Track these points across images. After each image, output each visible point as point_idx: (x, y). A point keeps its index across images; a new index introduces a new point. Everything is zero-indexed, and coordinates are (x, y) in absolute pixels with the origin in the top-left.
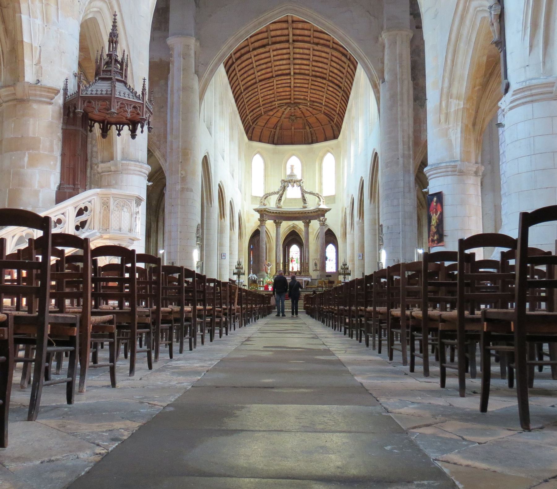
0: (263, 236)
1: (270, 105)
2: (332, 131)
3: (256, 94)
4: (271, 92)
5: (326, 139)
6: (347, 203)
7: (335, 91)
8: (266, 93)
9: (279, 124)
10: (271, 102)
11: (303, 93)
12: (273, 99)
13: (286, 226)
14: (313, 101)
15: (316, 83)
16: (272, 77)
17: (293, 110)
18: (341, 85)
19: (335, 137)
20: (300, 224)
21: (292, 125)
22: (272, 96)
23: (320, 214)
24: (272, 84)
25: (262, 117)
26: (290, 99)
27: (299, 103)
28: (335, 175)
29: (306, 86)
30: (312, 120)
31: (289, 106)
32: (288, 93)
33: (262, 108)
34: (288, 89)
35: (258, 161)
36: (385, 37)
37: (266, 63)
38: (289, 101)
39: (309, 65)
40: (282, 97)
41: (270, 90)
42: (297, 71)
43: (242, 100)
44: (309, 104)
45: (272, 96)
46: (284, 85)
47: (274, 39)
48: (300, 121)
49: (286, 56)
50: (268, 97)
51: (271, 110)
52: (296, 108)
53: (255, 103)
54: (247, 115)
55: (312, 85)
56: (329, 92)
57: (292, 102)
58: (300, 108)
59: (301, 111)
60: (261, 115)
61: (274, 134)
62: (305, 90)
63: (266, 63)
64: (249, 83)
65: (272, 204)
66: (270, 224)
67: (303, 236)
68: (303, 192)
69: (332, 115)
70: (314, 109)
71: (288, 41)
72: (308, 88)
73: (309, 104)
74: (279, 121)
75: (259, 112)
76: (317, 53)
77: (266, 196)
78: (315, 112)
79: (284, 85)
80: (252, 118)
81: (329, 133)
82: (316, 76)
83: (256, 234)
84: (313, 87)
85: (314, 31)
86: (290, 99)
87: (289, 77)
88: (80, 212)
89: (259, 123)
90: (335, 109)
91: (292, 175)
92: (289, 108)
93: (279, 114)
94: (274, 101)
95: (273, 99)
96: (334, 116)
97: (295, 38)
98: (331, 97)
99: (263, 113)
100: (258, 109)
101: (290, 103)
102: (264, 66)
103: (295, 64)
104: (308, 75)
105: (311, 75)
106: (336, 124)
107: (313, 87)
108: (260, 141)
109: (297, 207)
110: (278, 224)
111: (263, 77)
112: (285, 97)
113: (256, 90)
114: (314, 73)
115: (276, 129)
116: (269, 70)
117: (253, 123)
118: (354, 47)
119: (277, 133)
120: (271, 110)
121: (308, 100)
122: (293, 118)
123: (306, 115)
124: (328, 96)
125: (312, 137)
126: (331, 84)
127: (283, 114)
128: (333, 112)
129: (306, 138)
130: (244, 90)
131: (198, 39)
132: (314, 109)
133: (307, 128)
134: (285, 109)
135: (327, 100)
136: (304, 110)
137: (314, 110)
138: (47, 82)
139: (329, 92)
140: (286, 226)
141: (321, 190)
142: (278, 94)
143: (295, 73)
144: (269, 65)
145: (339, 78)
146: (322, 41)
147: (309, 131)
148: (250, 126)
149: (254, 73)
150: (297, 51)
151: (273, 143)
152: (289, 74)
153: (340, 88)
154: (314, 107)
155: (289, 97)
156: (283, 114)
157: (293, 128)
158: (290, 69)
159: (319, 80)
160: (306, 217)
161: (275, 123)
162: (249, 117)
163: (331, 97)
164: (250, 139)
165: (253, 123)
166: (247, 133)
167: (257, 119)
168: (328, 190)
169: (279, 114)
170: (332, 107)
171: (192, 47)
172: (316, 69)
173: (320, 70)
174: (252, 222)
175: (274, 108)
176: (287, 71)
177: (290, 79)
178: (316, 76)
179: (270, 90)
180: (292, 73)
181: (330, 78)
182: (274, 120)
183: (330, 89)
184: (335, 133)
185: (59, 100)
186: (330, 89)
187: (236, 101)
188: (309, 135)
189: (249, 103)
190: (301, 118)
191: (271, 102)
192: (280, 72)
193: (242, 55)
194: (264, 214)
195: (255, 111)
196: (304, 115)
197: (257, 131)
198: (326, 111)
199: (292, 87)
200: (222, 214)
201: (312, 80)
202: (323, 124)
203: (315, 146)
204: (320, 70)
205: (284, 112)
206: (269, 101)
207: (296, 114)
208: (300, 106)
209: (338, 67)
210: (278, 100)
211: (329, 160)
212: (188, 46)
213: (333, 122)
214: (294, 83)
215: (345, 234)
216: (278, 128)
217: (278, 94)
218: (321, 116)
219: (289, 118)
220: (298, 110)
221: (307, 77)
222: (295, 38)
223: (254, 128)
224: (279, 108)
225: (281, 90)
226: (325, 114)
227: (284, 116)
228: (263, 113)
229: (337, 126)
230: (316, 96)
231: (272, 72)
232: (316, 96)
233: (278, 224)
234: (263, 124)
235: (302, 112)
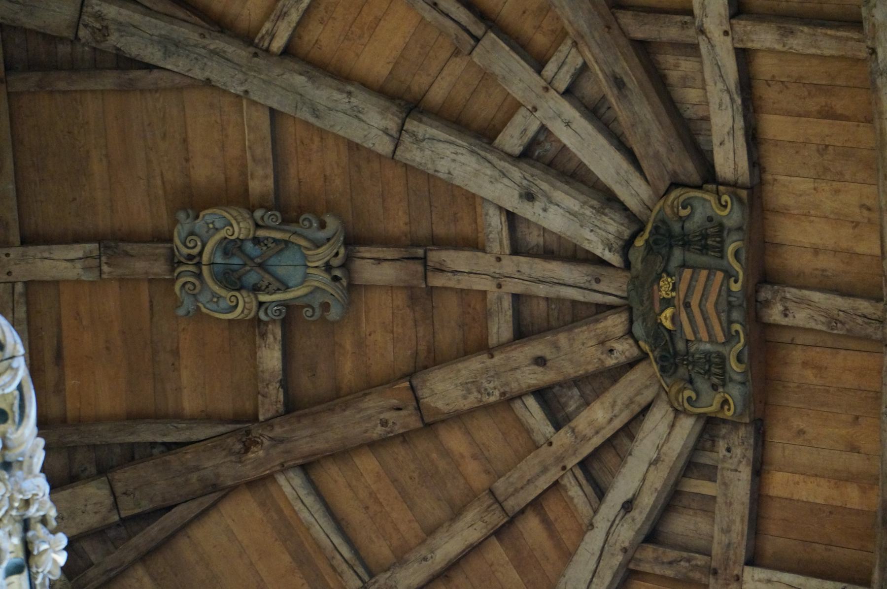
21: (112, 242)
122: (304, 273)
134: (543, 158)
156: (411, 106)
157: (60, 263)
190: (292, 407)
227: (373, 126)
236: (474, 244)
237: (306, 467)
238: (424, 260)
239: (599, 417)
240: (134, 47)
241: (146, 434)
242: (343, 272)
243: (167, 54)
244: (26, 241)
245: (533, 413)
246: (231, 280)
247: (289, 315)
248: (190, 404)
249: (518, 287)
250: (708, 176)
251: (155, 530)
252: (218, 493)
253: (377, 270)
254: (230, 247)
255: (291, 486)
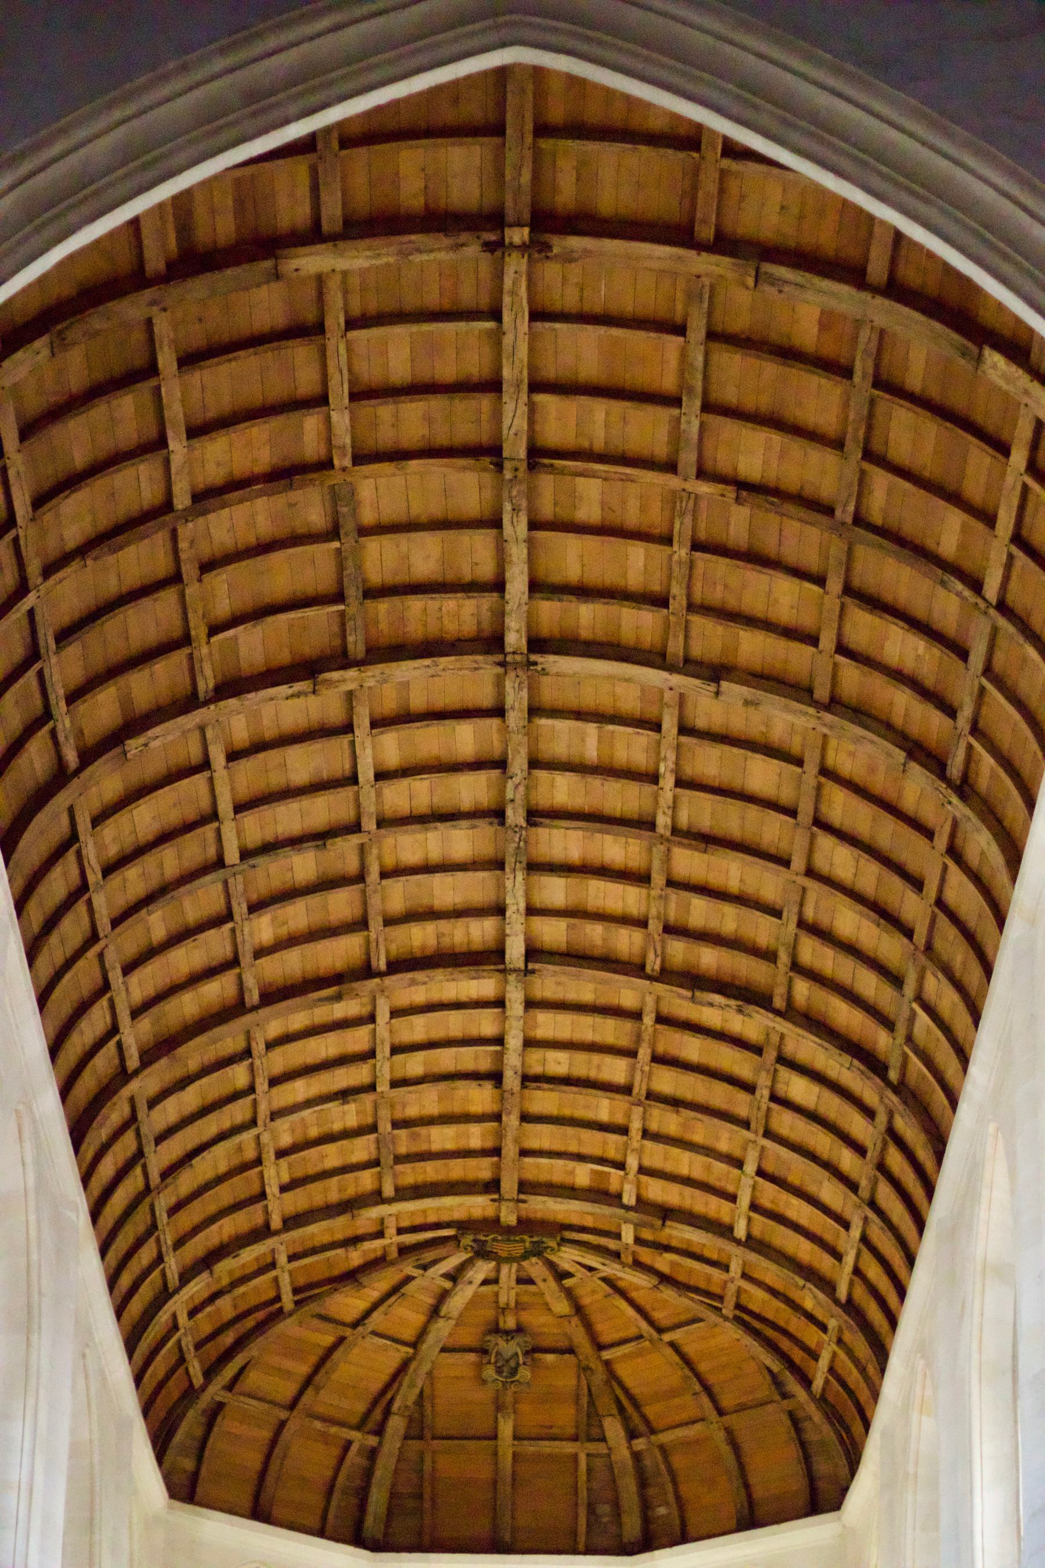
1: (339, 1227)
2: (793, 1451)
3: (238, 1112)
4: (348, 1115)
5: (751, 1518)
7: (832, 1106)
8: (311, 1122)
9: (406, 1396)
10: (348, 1206)
11: (592, 1142)
12: (366, 1180)
14: (666, 1213)
15: (692, 1048)
16: (366, 971)
17: (508, 1291)
18: (882, 1041)
22: (361, 1149)
24: (357, 1039)
25: (287, 1327)
26: (492, 1186)
27: (560, 1230)
29: (615, 1070)
30: (646, 1371)
31: (482, 1253)
32: (476, 1136)
33: (279, 1246)
34: (479, 1097)
37: (321, 837)
38: (478, 1205)
39: (641, 878)
40: (430, 1171)
41: (344, 1095)
42: (553, 932)
43: (127, 1144)
44: (628, 1234)
45: (361, 1149)
46: (447, 1059)
47: (383, 607)
48: (560, 1375)
49: (471, 789)
50: (331, 1156)
51: (351, 1277)
52: (535, 1268)
53: (225, 1194)
54: (165, 1294)
55: (658, 1059)
56: (786, 1123)
57: (509, 1217)
58: (561, 1276)
59: (569, 1294)
60: (271, 1313)
61: (368, 1474)
62: (604, 1108)
63: (321, 837)
64: (187, 1006)
69: (796, 1324)
70: (665, 1279)
71: (491, 642)
72: (626, 1090)
73: (628, 1234)
74: (404, 1367)
75: (260, 1287)
76: (710, 762)
78: (670, 1303)
79: (447, 1059)
80: (205, 1323)
81: (775, 1468)
82: (694, 981)
84: (667, 1081)
85: (697, 546)
86: (492, 1186)
87: (484, 986)
89: (254, 1379)
90: (824, 1263)
92: (483, 1269)
93: (406, 1316)
94: (377, 1197)
95: (366, 1180)
96: (811, 1336)
97: (551, 613)
98: (799, 1170)
99: (288, 1300)
100: (249, 1255)
101: (493, 1224)
102: (303, 866)
103: (535, 867)
104: (636, 969)
105: (653, 964)
106: (822, 1401)
107: (667, 1081)
108: (259, 1511)
111: (292, 964)
112: (457, 1170)
113: (238, 1075)
114: (678, 950)
115: (379, 1431)
116: (340, 904)
117: (209, 1373)
119: (383, 1472)
120: (351, 1277)
121: (629, 1199)
122: (509, 1348)
123: (607, 1333)
124: (782, 1159)
125: (646, 1506)
126: (807, 1047)
127: (435, 1312)
128: (811, 1298)
129: (604, 1509)
130: (149, 1056)
132: (665, 1279)
133: (613, 1429)
134: (453, 1277)
135: (770, 1195)
136: (592, 1291)
137: (668, 1294)
139: (786, 1123)
142: (404, 1142)
143: (534, 953)
144: (343, 853)
145: (868, 984)
146: (753, 647)
147: (622, 1453)
148: (190, 1393)
149: (227, 916)
150: (562, 737)
152: (491, 957)
153: (873, 1063)
154: (664, 1262)
155: (481, 1169)
156: (435, 1312)
157: (506, 1429)
158: (499, 910)
159: (716, 1012)
161: (376, 1386)
162: (178, 1305)
163: (799, 1170)
164: (185, 1489)
165: (209, 1373)
166: (161, 1443)
167: (240, 1344)
169: (406, 1316)
170: (804, 1250)
172: (700, 912)
173: (729, 919)
175: (378, 1263)
176: (478, 932)
177: (499, 1003)
178: (694, 981)
179: (344, 1095)
180: (515, 951)
181: (802, 989)
182: (367, 1363)
183: (799, 1089)
184: (822, 1467)
186: (799, 1089)
187: (78, 1131)
188: (629, 1487)
189: (186, 1182)
190: (571, 1351)
191: (348, 1206)
192: (421, 936)
193: (135, 724)
195: (226, 1268)
196: (588, 1326)
197: (240, 1440)
198: (758, 1299)
199: (511, 1080)
201: (662, 1019)
202: (727, 1401)
204: (729, 919)
205: (443, 1296)
206: (332, 1191)
207: (528, 1318)
208: (567, 1257)
209: (868, 876)
210: (404, 1193)
213: (806, 1382)
214: (529, 1043)
216: (396, 1424)
217: (404, 1142)
218: (720, 1342)
219: (484, 1351)
220: (549, 1287)
221: (627, 992)
222: (551, 613)
223: (216, 1410)
224: (408, 1268)
225: (426, 1101)
226: (748, 1320)
227: (441, 1330)
228: (288, 1300)
229: (833, 1415)
230: (685, 1163)
231: (361, 924)
232: (685, 1163)
234: (287, 1390)
235: (579, 1309)
236: (497, 1295)
237: (601, 1347)
238: (503, 1309)
239: (566, 1266)
240: (413, 1396)
241: (585, 1400)
242: (508, 1334)
243: (414, 1386)
244: (495, 1437)
245: (568, 1282)
246: (514, 1371)
247: (527, 1353)
248: (574, 1382)
249: (513, 1283)
250: (454, 1238)
251: (625, 1402)
252: (612, 1376)
253: (510, 1322)
254: (499, 1371)
255: (606, 1355)
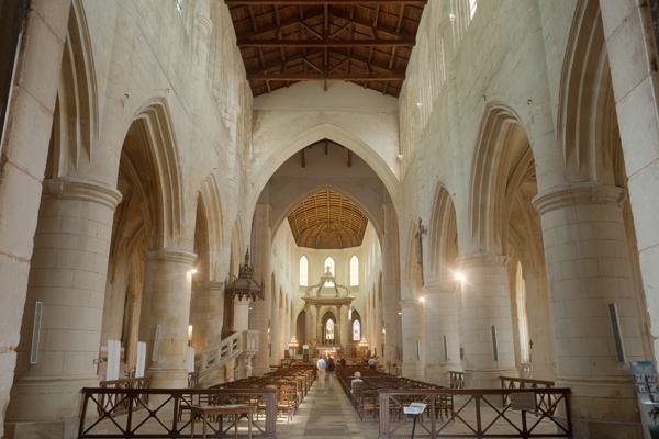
0: (308, 316)
6: (366, 295)
13: (324, 309)
19: (359, 245)
20: (334, 307)
23: (348, 302)
28: (357, 270)
30: (342, 232)
35: (304, 262)
36: (384, 207)
65: (314, 294)
66: (313, 308)
67: (336, 314)
68: (336, 286)
77: (310, 288)
83: (303, 313)
88: (235, 341)
91: (329, 273)
109: (332, 295)
110: (318, 308)
118: (364, 210)
131: (271, 205)
138: (219, 280)
140: (324, 309)
141: (349, 282)
151: (315, 248)
160: (339, 303)
164: (299, 245)
168: (354, 281)
171: (268, 210)
174: (300, 305)
182: (316, 232)
185: (223, 287)
194: (308, 301)
197: (304, 240)
200: (281, 306)
203: (345, 250)
211: (354, 261)
212: (264, 210)
215: (365, 315)
233: (318, 308)
